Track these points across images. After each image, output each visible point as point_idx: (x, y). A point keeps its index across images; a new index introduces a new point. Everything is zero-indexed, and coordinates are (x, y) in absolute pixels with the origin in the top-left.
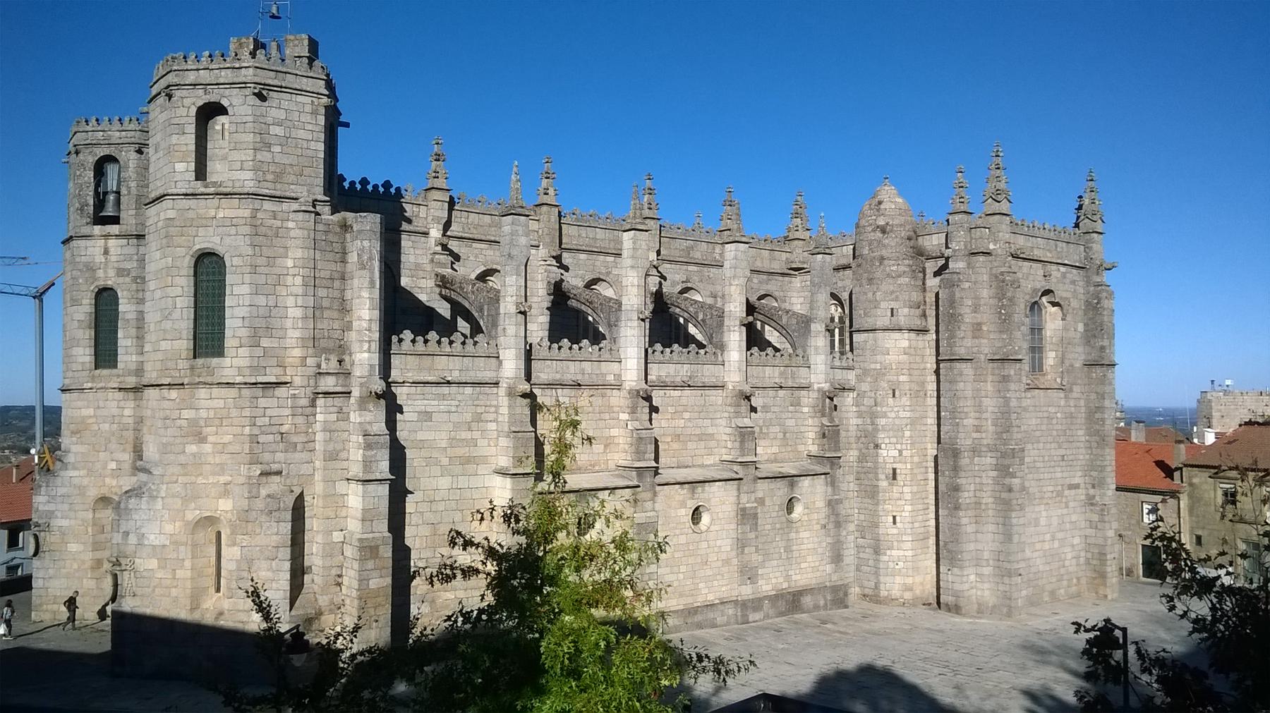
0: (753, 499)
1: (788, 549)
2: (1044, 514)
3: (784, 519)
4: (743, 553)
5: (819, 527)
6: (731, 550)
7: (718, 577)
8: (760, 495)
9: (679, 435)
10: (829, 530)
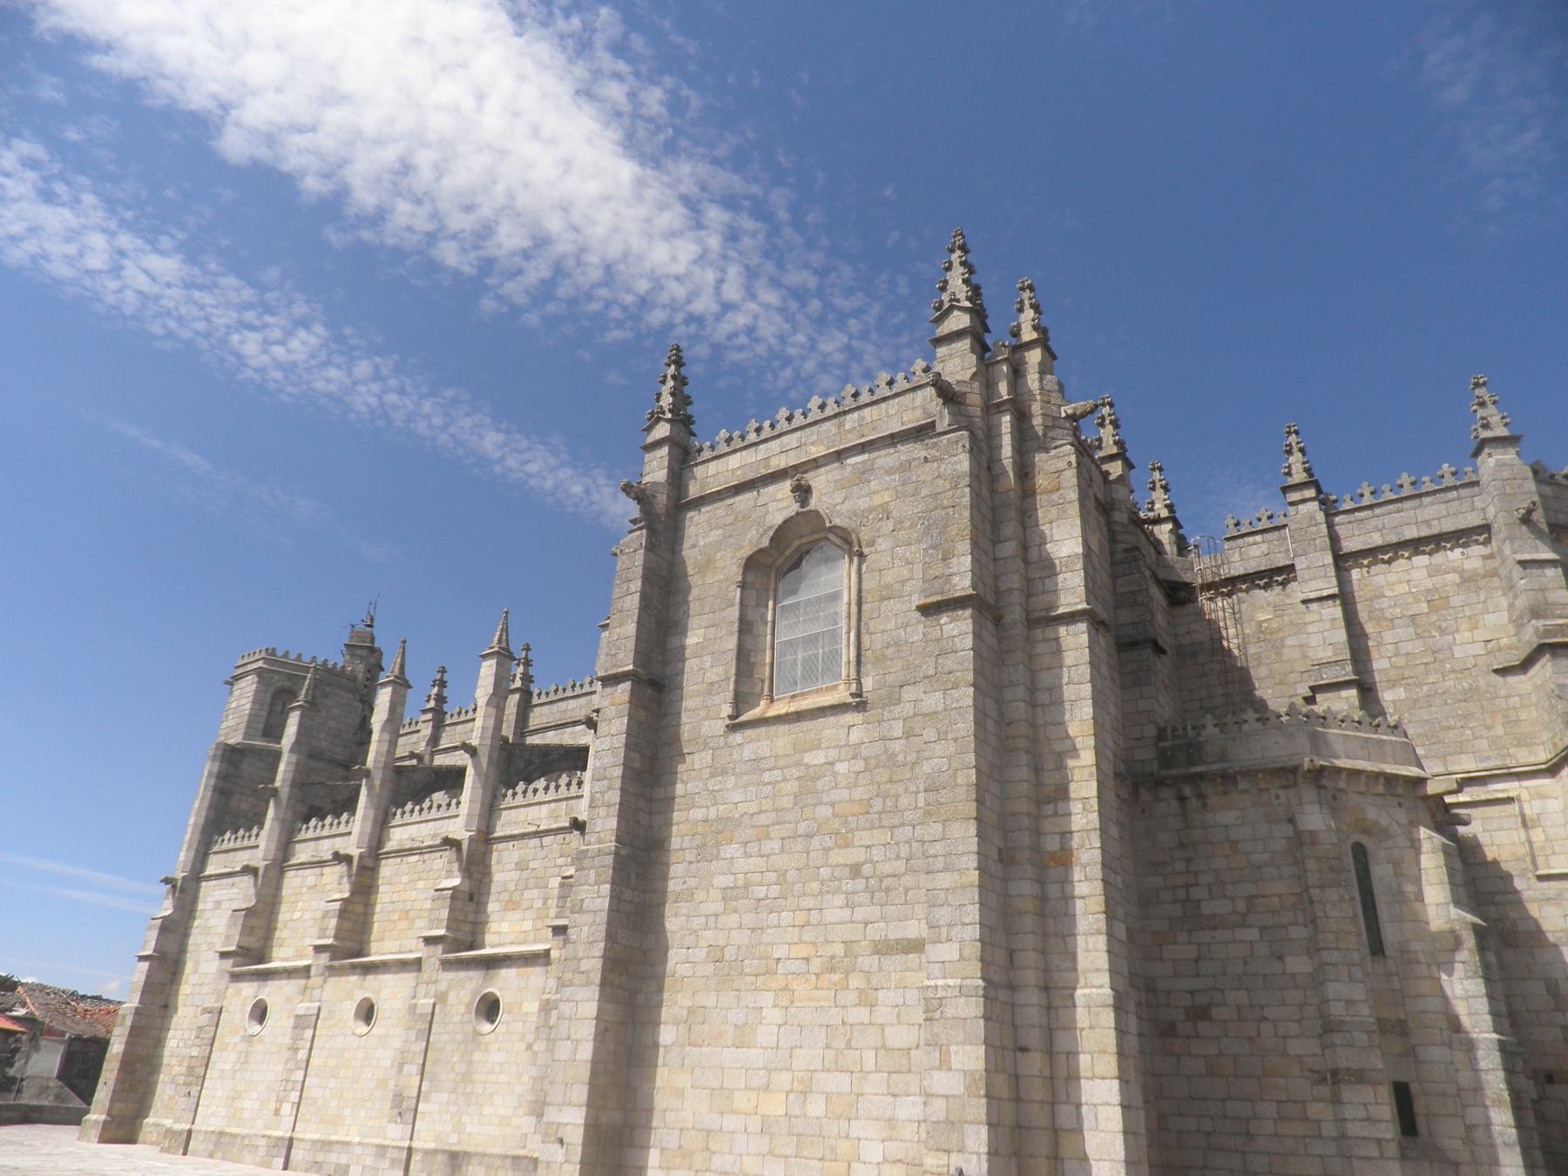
0: (432, 993)
1: (467, 1077)
2: (773, 1015)
3: (469, 1028)
4: (400, 1071)
5: (522, 1046)
6: (392, 1066)
7: (369, 1104)
8: (443, 986)
9: (408, 911)
10: (535, 1054)
